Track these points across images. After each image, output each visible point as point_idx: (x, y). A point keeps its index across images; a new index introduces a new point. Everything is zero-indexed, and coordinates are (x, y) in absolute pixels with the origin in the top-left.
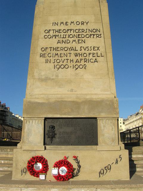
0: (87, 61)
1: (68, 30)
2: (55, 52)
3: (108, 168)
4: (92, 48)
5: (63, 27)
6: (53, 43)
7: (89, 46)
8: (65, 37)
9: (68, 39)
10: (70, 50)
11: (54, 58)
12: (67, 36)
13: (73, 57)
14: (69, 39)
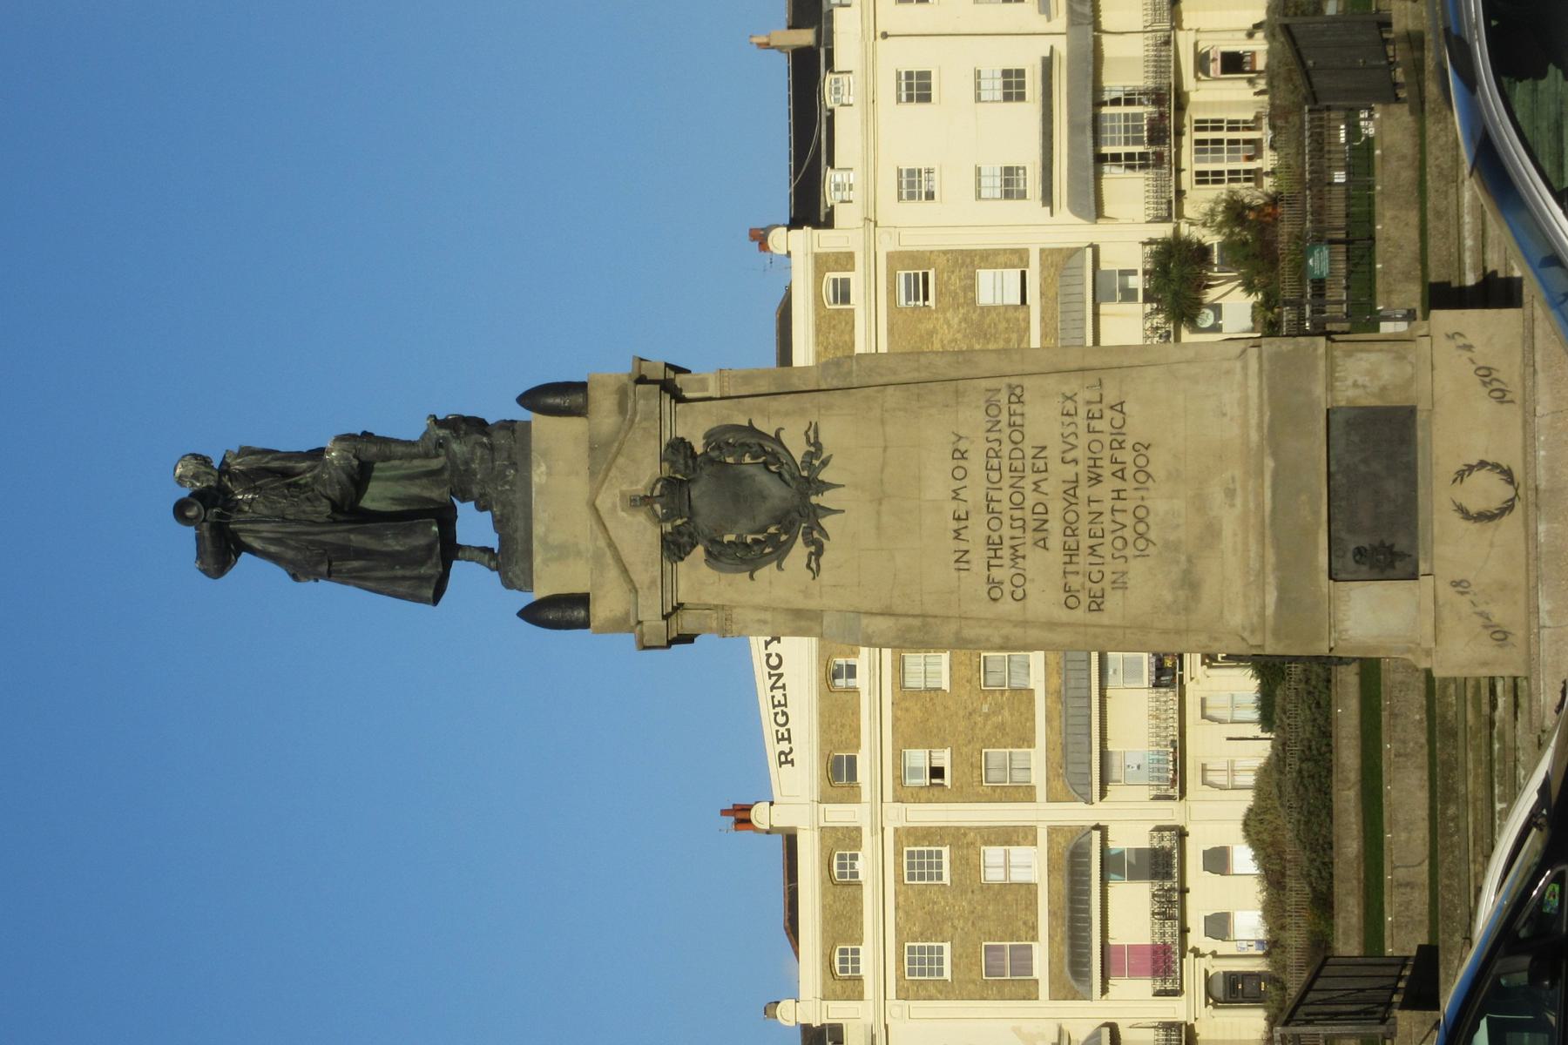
0: (1120, 438)
1: (990, 511)
2: (1083, 559)
3: (1486, 375)
4: (1068, 420)
5: (978, 529)
6: (1044, 566)
7: (1058, 429)
8: (1020, 523)
9: (1028, 512)
10: (1073, 500)
11: (1108, 558)
12: (1018, 514)
13: (1104, 491)
14: (1029, 504)
